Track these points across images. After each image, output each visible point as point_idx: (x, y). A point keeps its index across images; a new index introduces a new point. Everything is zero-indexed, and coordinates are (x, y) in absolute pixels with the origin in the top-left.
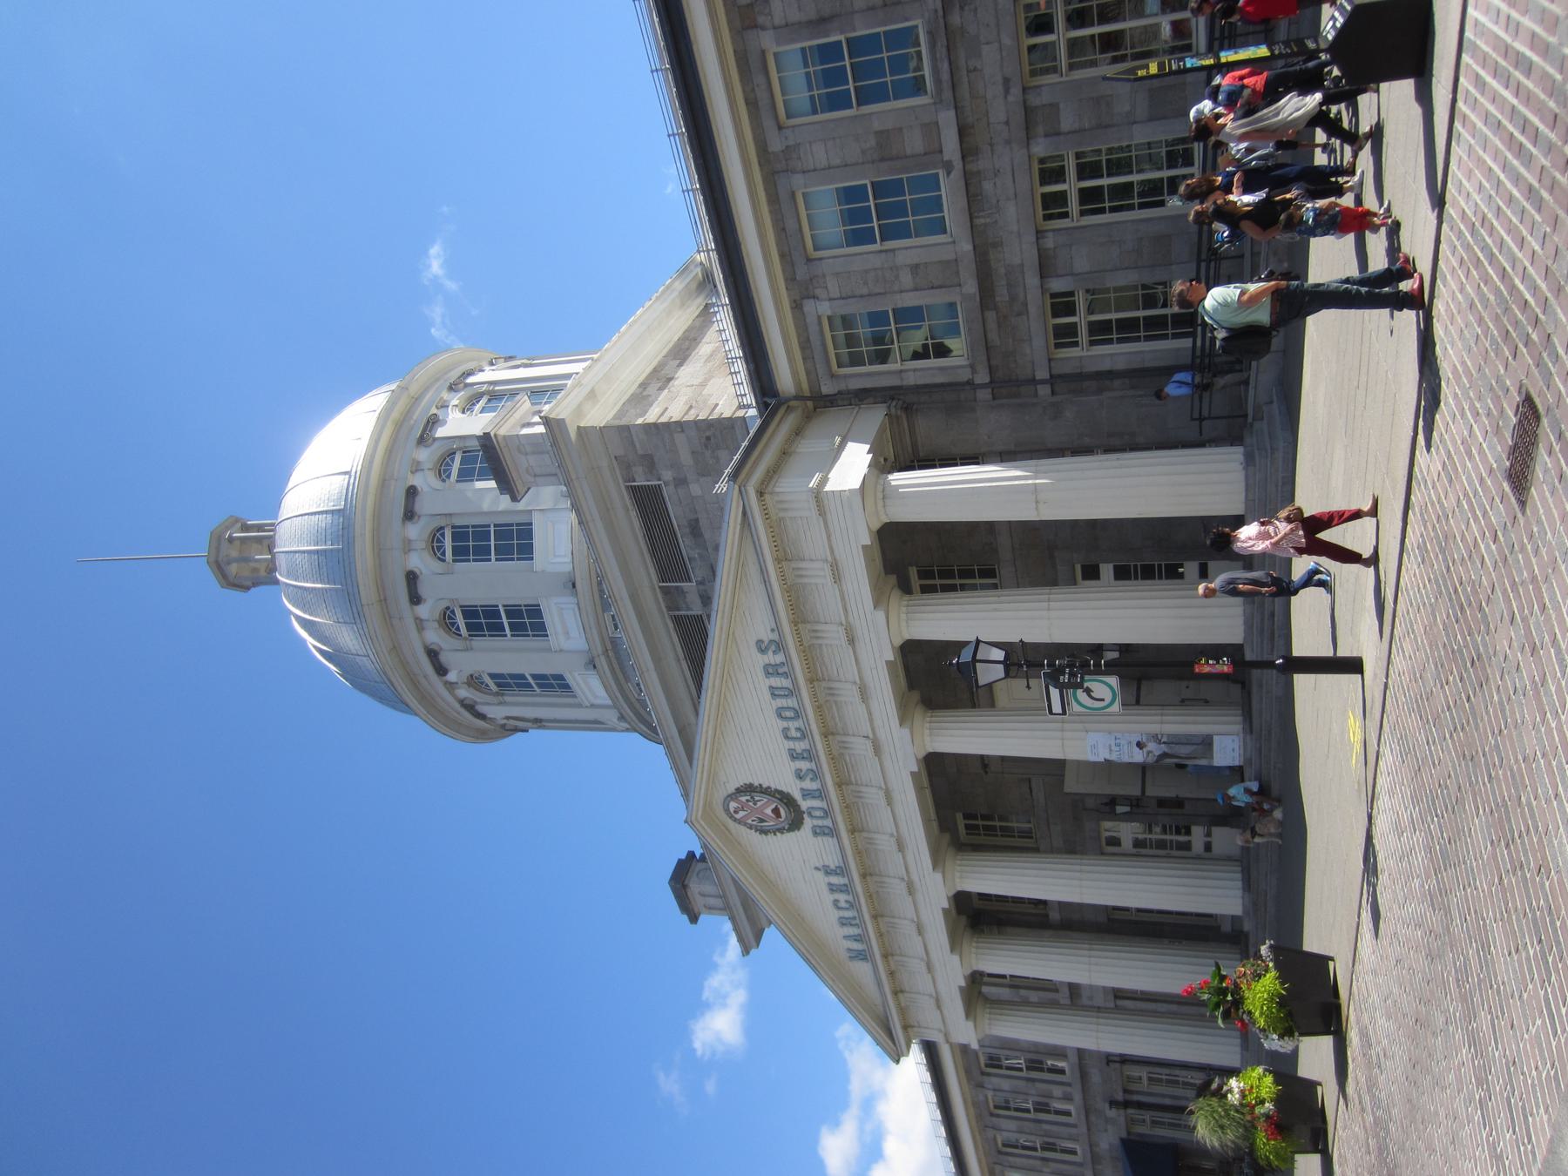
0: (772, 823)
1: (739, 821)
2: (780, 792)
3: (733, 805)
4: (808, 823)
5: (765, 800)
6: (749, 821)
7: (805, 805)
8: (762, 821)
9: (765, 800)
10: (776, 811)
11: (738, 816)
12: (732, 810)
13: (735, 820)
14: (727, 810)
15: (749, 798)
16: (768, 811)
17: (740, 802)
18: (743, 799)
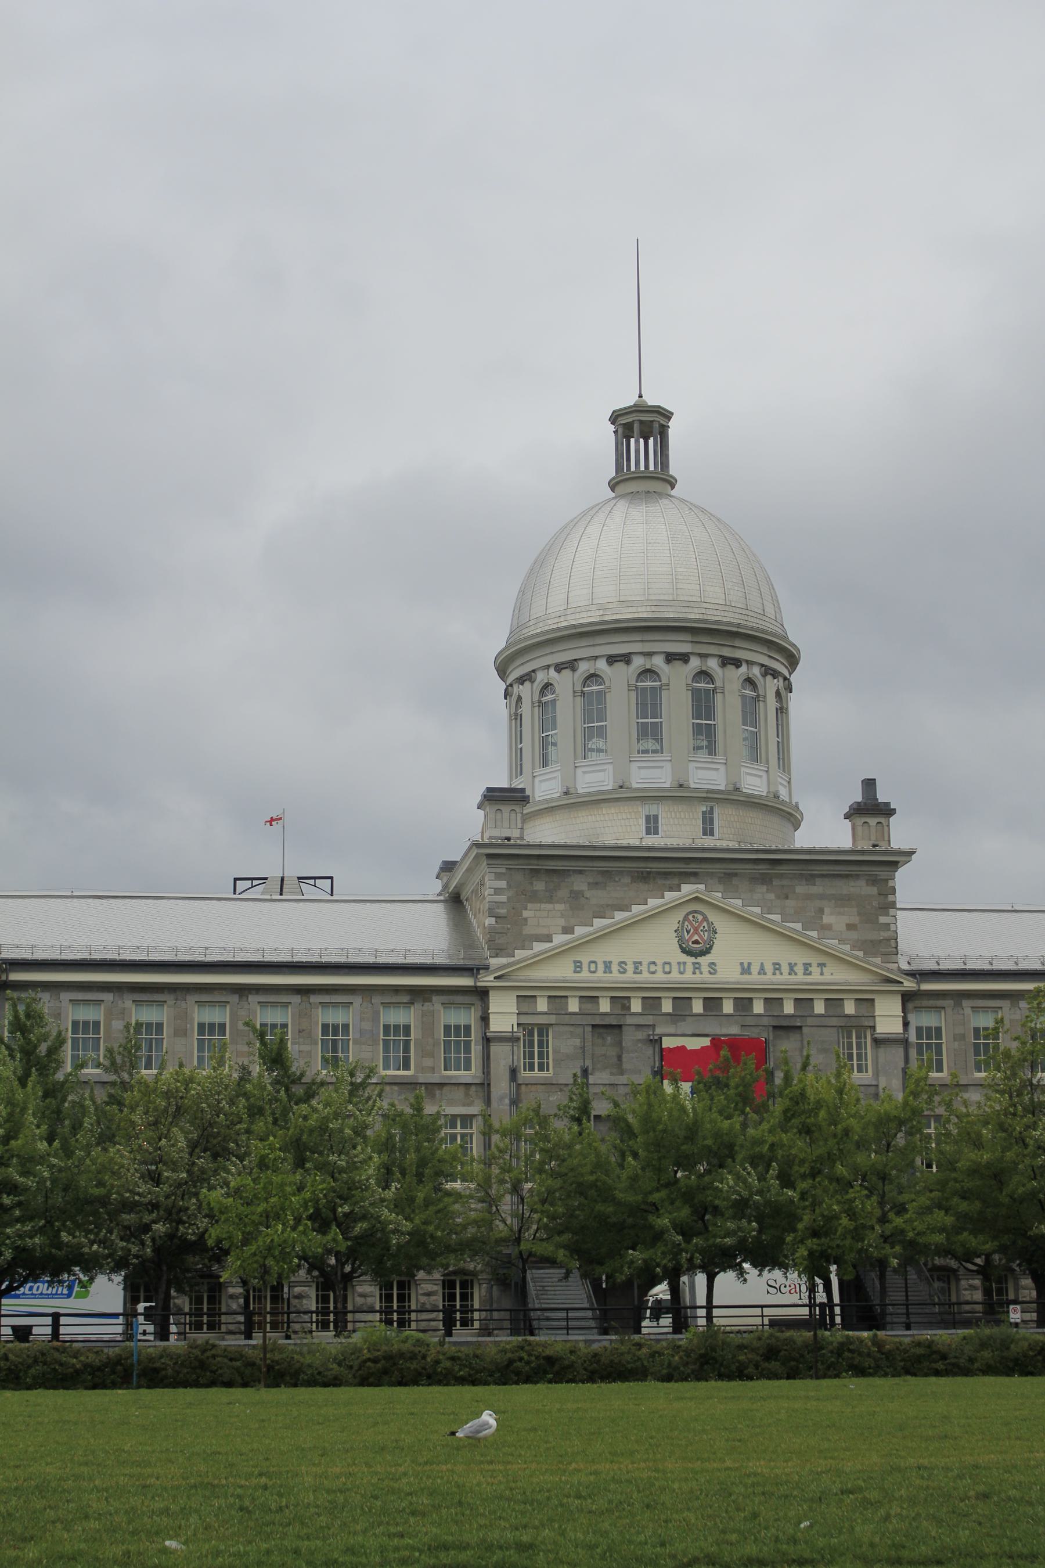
0: (687, 938)
1: (686, 918)
2: (711, 947)
3: (700, 918)
4: (690, 960)
5: (705, 938)
6: (686, 923)
7: (704, 961)
8: (688, 932)
9: (705, 938)
10: (696, 942)
11: (690, 917)
12: (696, 915)
13: (687, 914)
14: (695, 912)
15: (706, 928)
16: (696, 937)
17: (702, 921)
18: (705, 924)
